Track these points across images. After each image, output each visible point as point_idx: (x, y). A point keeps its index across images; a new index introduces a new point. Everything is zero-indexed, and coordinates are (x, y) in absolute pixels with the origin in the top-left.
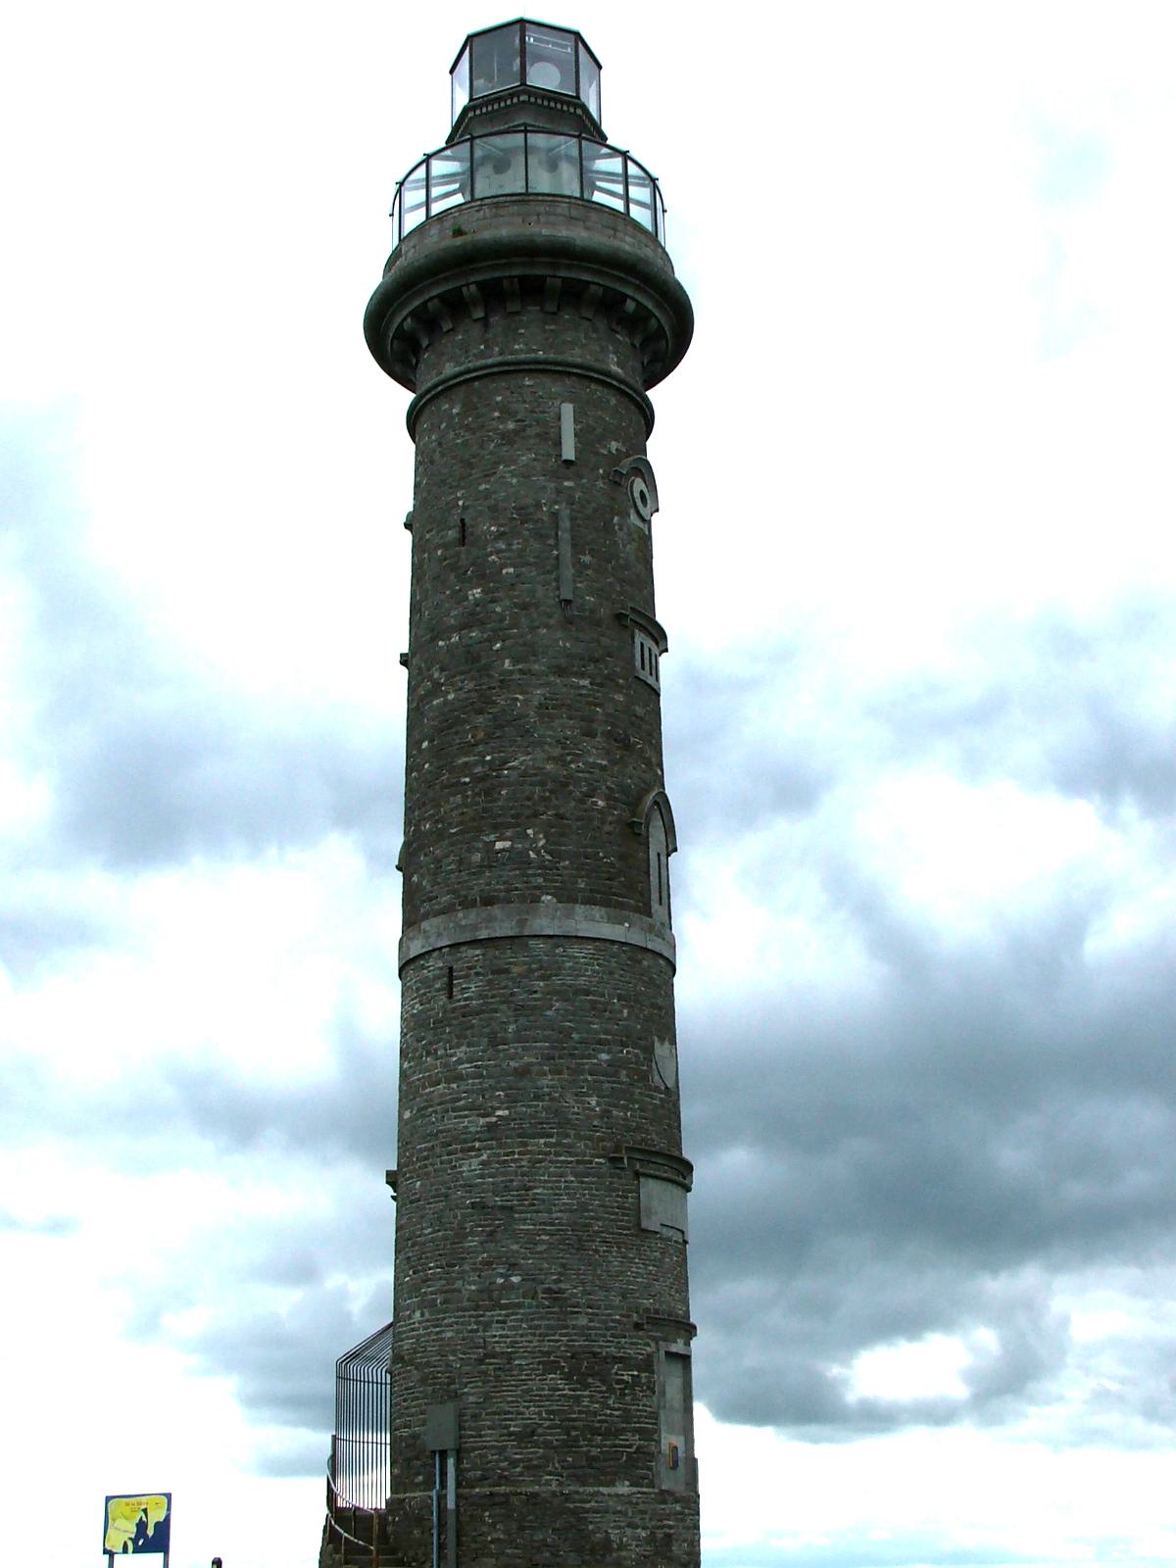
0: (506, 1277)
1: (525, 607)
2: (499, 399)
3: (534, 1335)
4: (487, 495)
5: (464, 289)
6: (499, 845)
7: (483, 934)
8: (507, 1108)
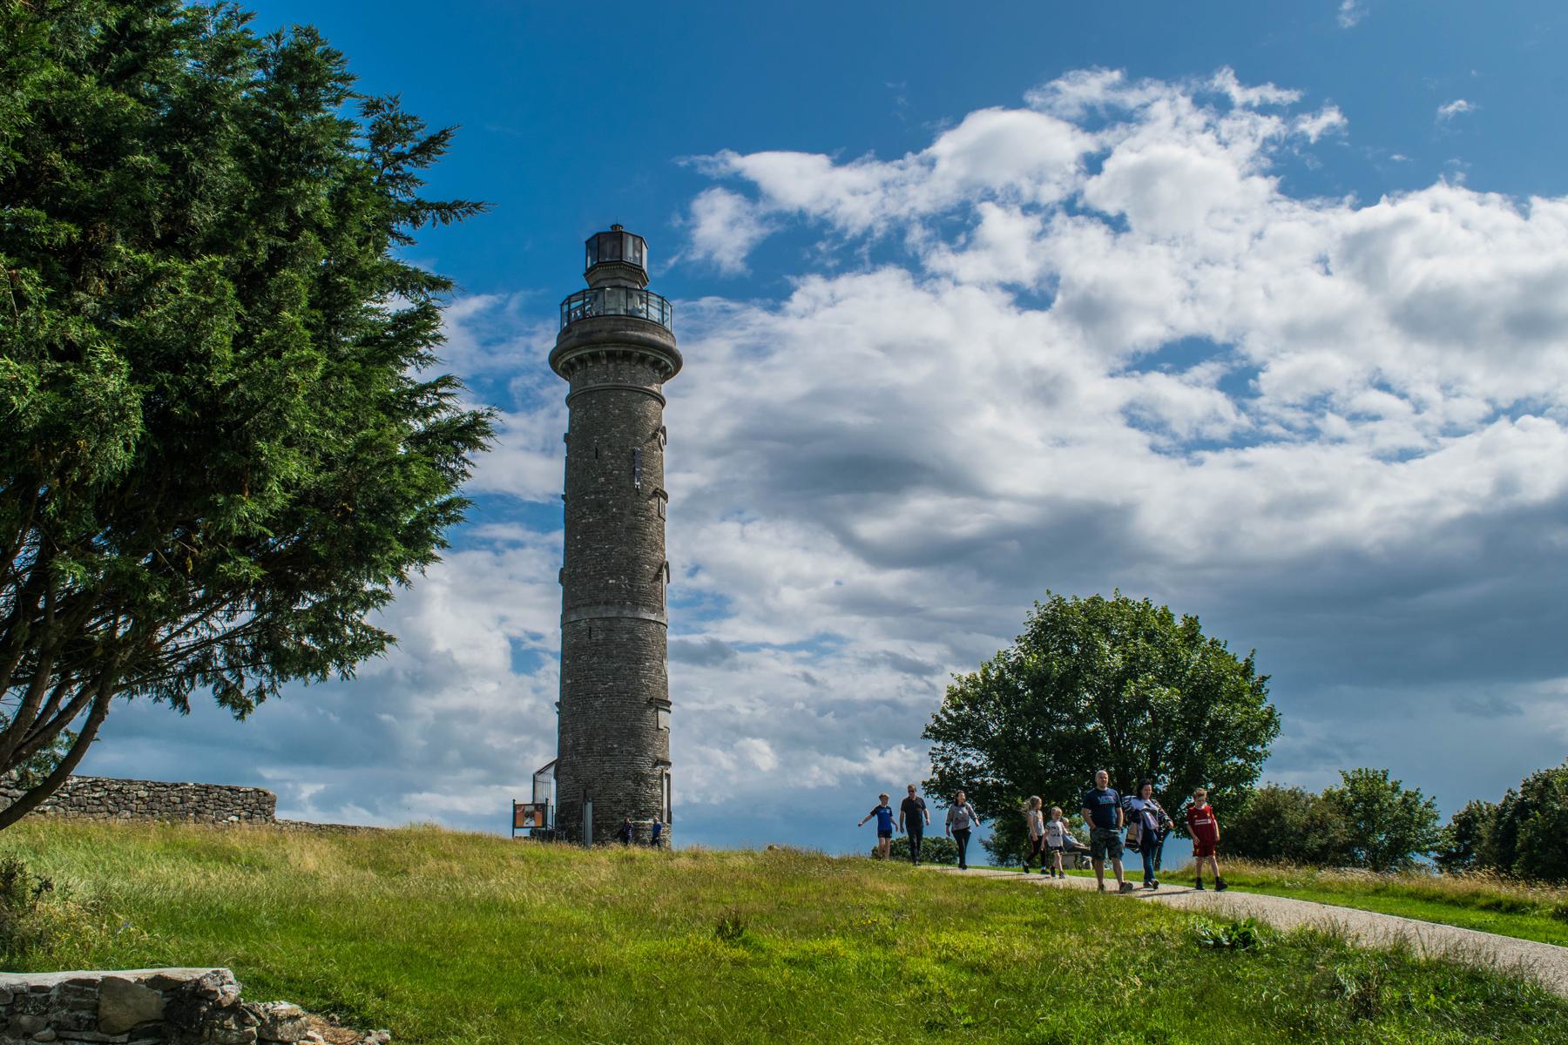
1: (621, 487)
4: (607, 440)
7: (604, 616)
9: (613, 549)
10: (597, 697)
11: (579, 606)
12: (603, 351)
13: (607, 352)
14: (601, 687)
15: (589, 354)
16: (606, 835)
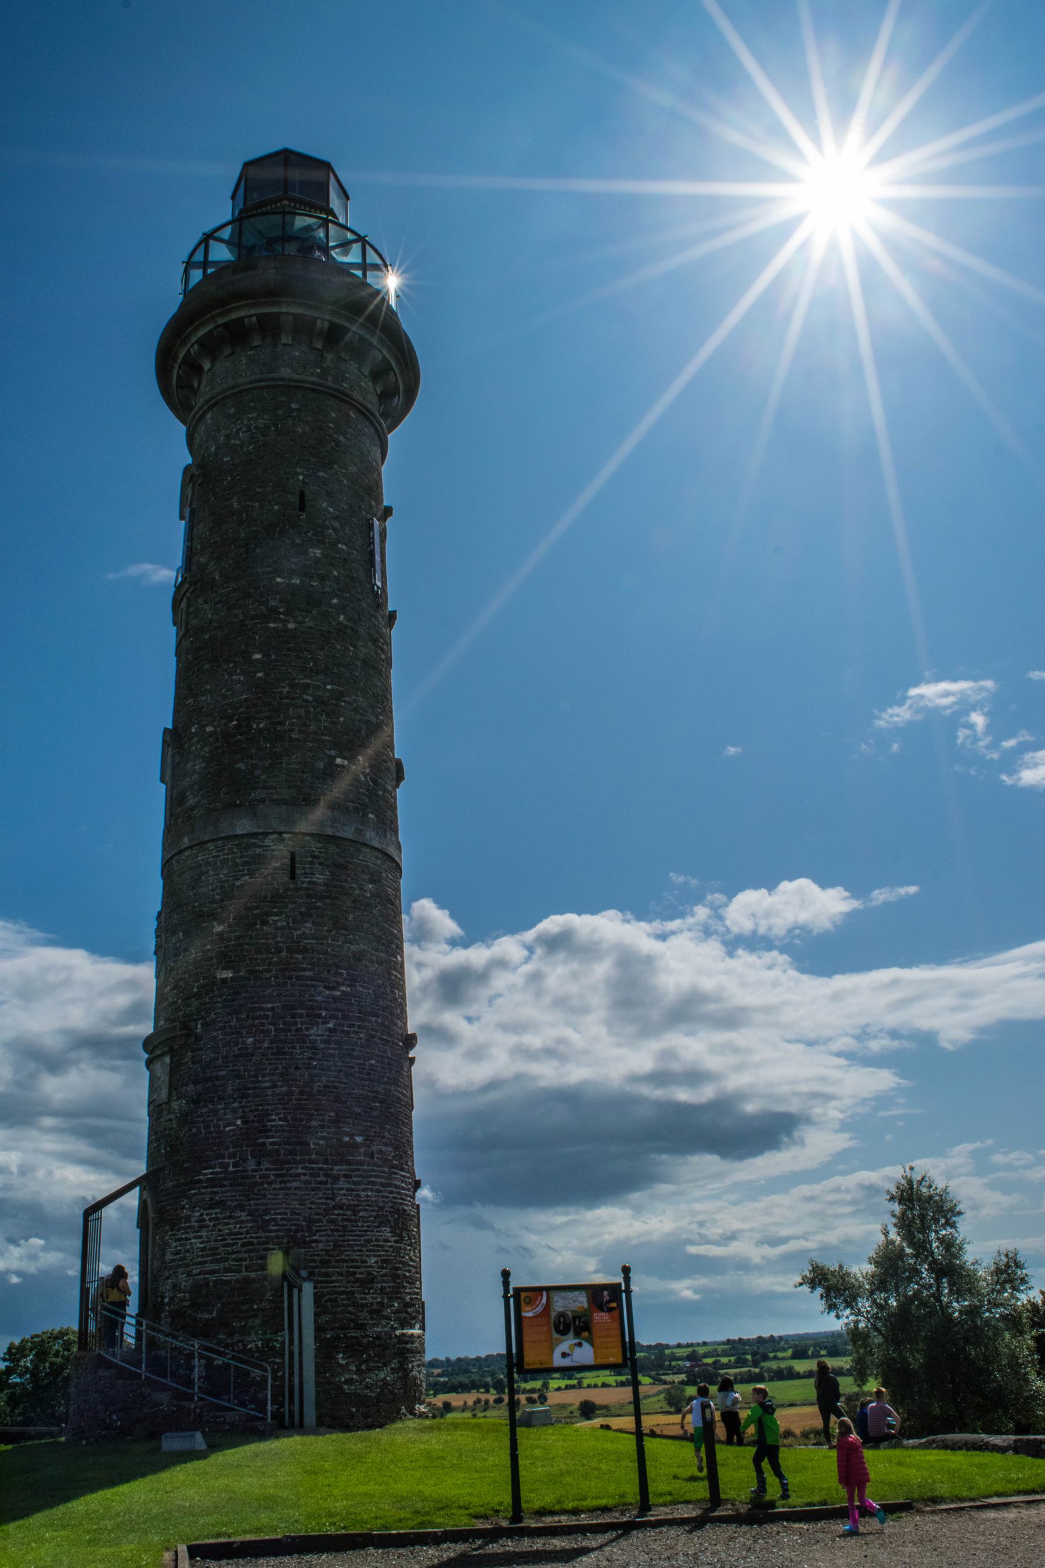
0: (352, 1136)
2: (334, 415)
3: (372, 1190)
5: (319, 322)
7: (329, 831)
8: (349, 986)
10: (313, 1018)
11: (262, 801)
14: (323, 994)
16: (345, 1368)
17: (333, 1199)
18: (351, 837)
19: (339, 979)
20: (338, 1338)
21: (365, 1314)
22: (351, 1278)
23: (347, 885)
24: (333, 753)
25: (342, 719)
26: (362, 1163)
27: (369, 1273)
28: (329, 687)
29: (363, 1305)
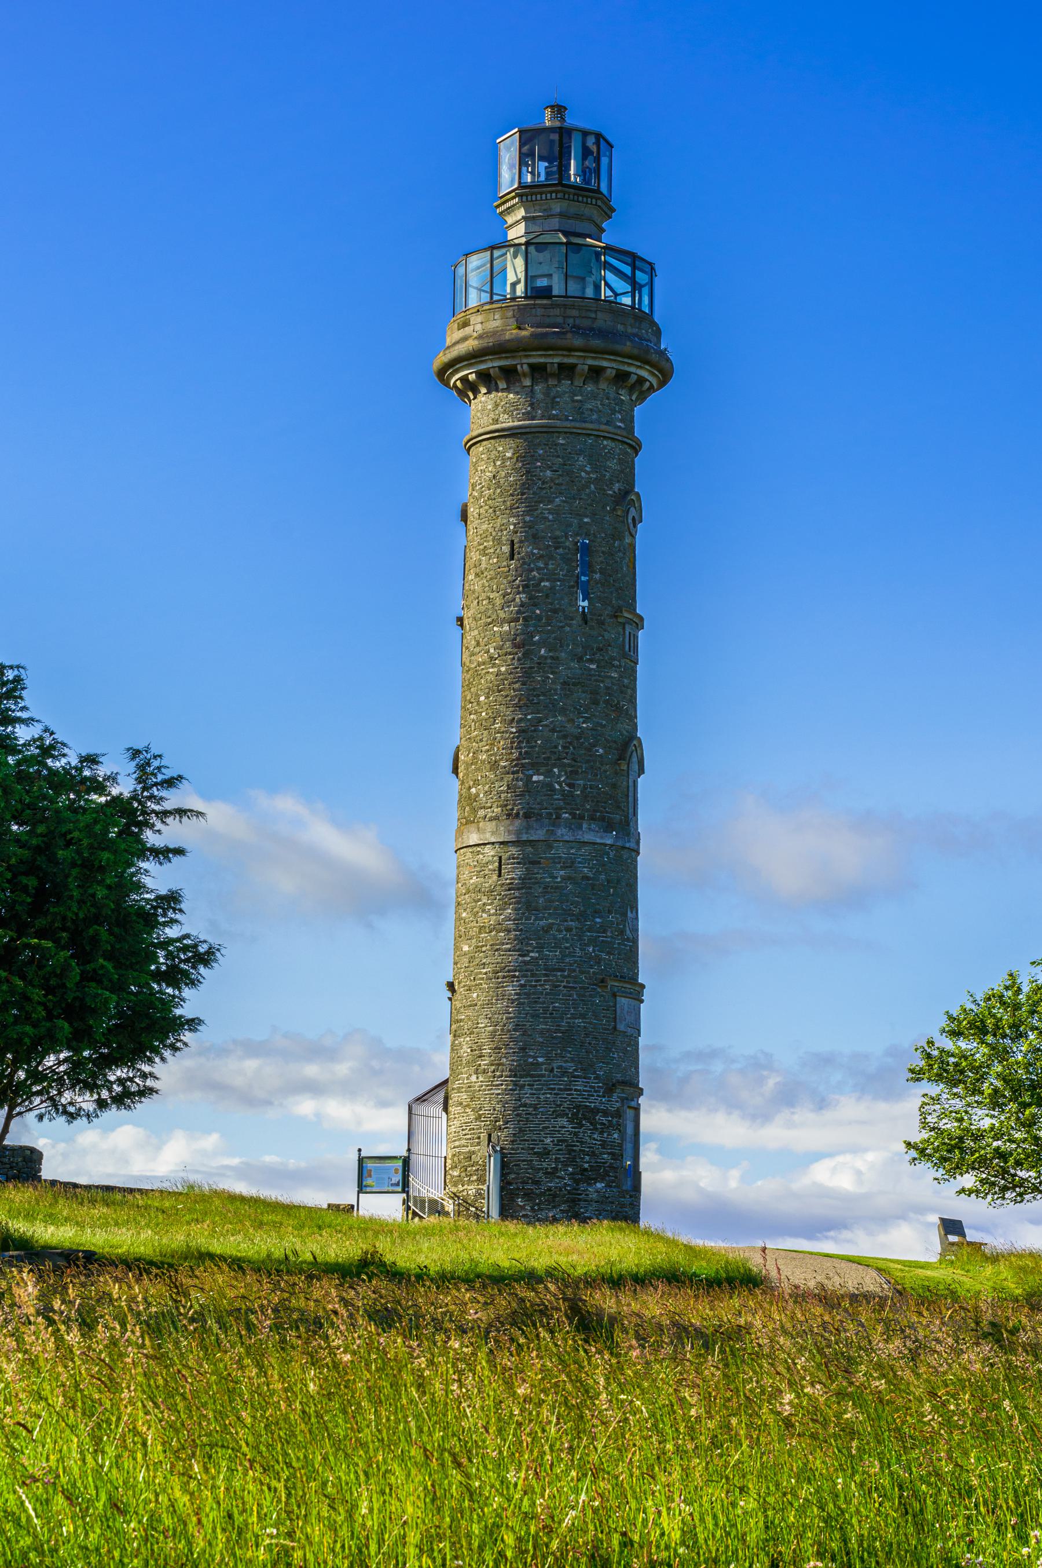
0: (535, 1057)
1: (555, 611)
3: (551, 1094)
5: (519, 367)
6: (535, 778)
7: (524, 837)
8: (537, 952)
9: (540, 720)
12: (523, 364)
13: (531, 366)
15: (500, 368)
16: (523, 1208)
17: (520, 1100)
18: (542, 838)
19: (529, 948)
20: (518, 1189)
21: (540, 1174)
22: (530, 1152)
23: (539, 876)
24: (531, 772)
25: (539, 742)
26: (543, 1076)
27: (545, 1149)
28: (529, 717)
29: (539, 1169)
